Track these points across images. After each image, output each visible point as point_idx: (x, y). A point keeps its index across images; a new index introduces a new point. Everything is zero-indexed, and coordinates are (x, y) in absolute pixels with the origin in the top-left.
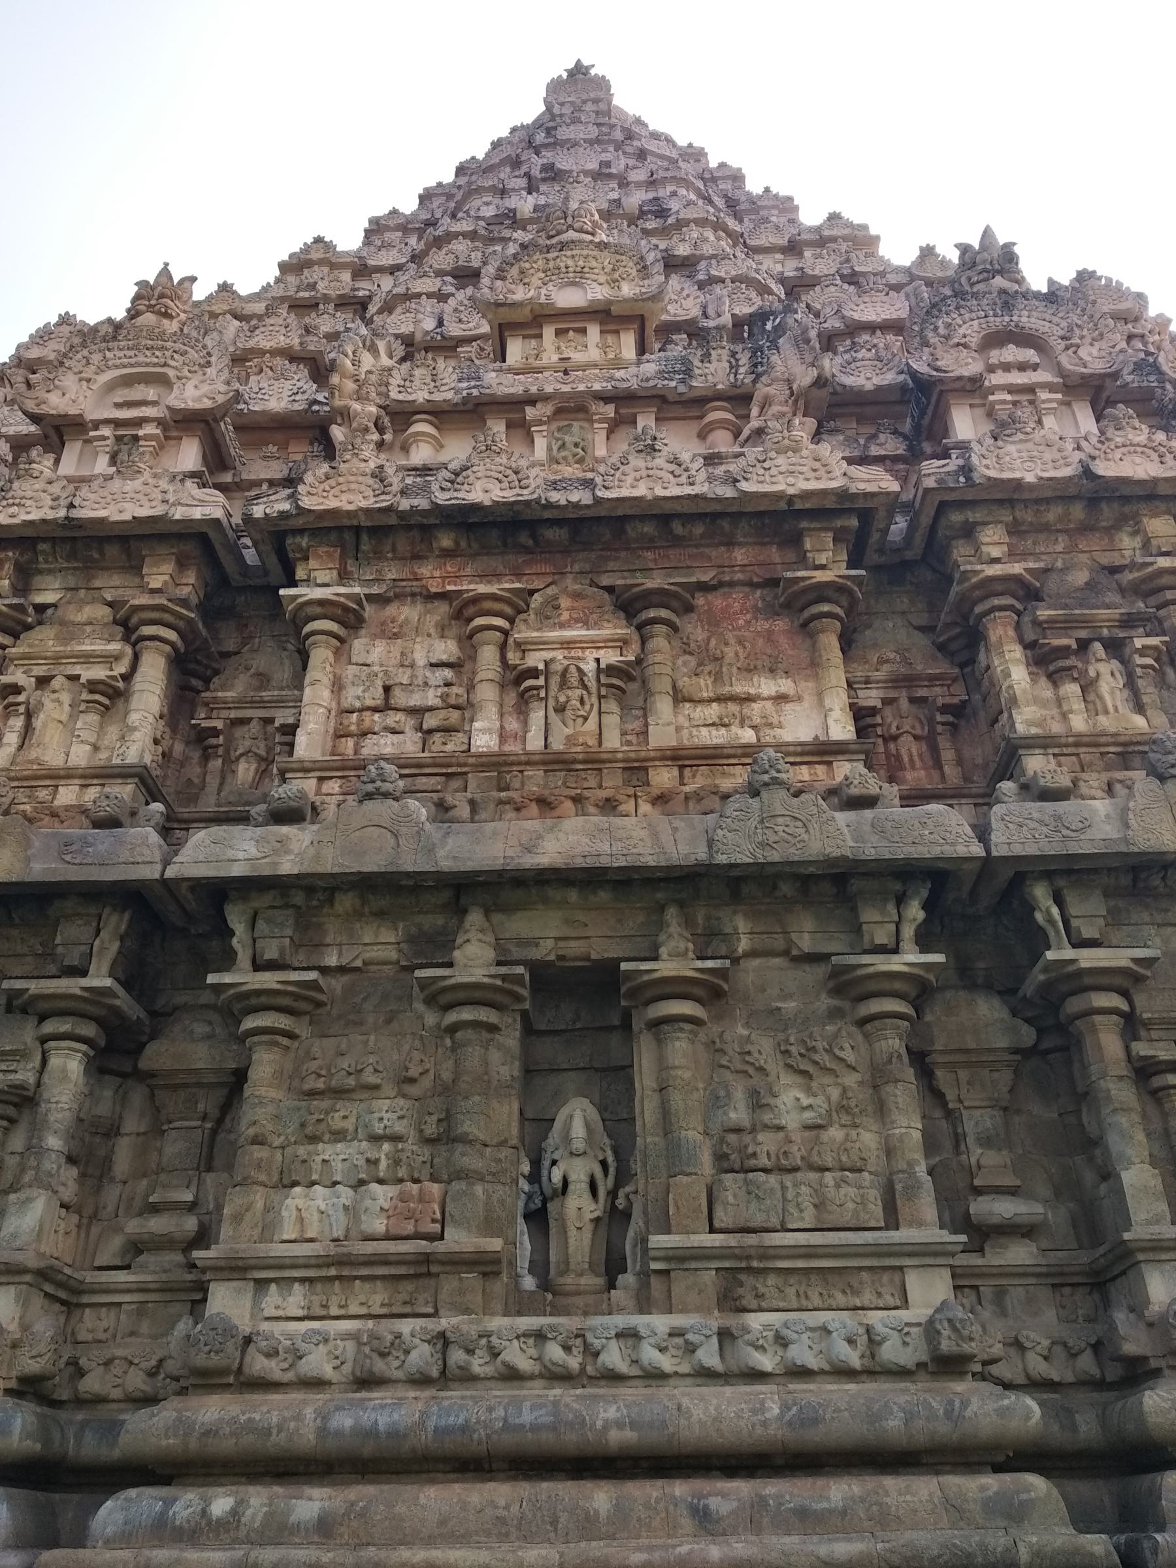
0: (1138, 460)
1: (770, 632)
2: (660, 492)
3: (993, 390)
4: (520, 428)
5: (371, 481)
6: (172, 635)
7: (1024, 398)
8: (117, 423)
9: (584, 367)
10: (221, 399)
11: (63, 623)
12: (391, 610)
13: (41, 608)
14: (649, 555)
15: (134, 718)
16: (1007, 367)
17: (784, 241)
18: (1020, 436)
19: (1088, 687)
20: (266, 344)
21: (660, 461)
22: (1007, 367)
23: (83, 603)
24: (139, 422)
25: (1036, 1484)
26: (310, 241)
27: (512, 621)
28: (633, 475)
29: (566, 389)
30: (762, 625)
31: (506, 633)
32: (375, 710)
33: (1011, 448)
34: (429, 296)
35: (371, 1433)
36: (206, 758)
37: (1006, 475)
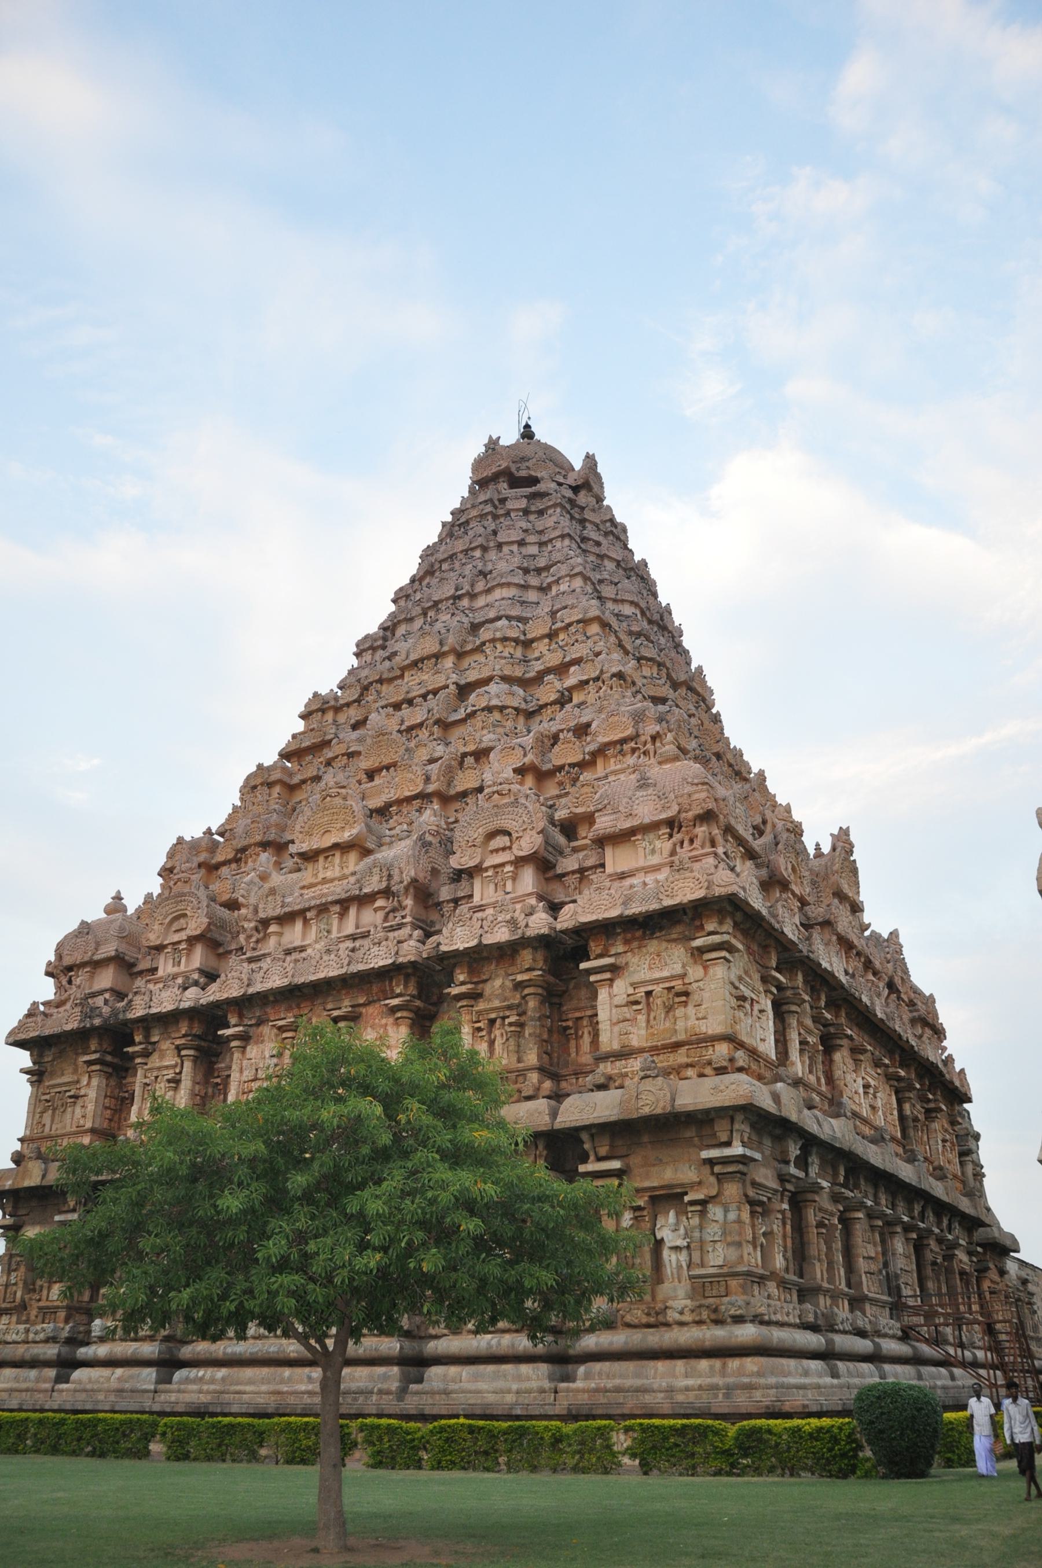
0: (504, 929)
1: (386, 1025)
2: (331, 974)
3: (486, 869)
4: (306, 922)
5: (237, 981)
6: (191, 1052)
7: (499, 870)
8: (174, 944)
9: (332, 880)
10: (204, 927)
11: (161, 1050)
12: (261, 1028)
13: (155, 1043)
14: (344, 992)
15: (182, 1092)
16: (497, 851)
17: (547, 631)
18: (461, 923)
19: (492, 1043)
20: (252, 841)
21: (333, 956)
22: (497, 851)
23: (166, 1039)
24: (179, 942)
25: (396, 1369)
26: (311, 696)
27: (295, 1031)
28: (324, 964)
29: (318, 902)
30: (384, 1021)
31: (293, 1038)
32: (252, 1081)
33: (458, 929)
34: (343, 755)
35: (235, 1354)
36: (220, 1094)
37: (451, 948)
